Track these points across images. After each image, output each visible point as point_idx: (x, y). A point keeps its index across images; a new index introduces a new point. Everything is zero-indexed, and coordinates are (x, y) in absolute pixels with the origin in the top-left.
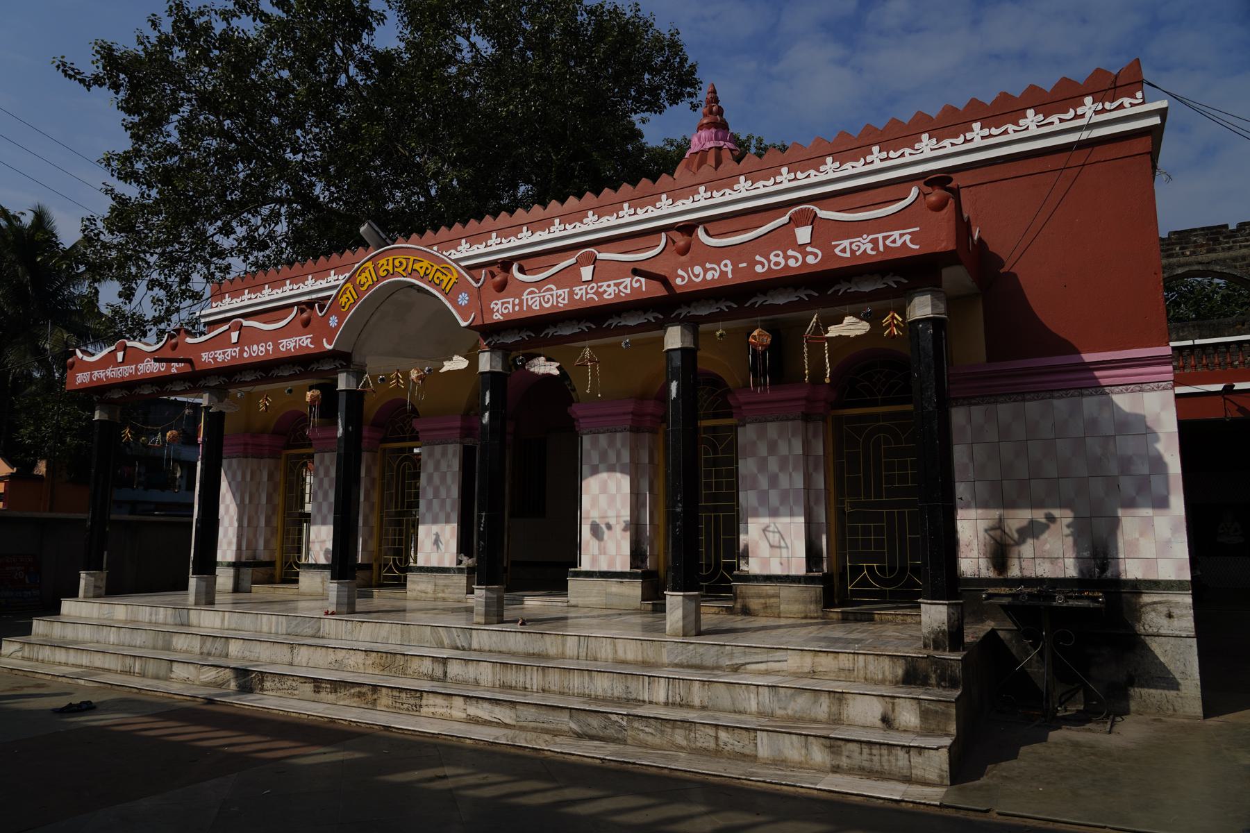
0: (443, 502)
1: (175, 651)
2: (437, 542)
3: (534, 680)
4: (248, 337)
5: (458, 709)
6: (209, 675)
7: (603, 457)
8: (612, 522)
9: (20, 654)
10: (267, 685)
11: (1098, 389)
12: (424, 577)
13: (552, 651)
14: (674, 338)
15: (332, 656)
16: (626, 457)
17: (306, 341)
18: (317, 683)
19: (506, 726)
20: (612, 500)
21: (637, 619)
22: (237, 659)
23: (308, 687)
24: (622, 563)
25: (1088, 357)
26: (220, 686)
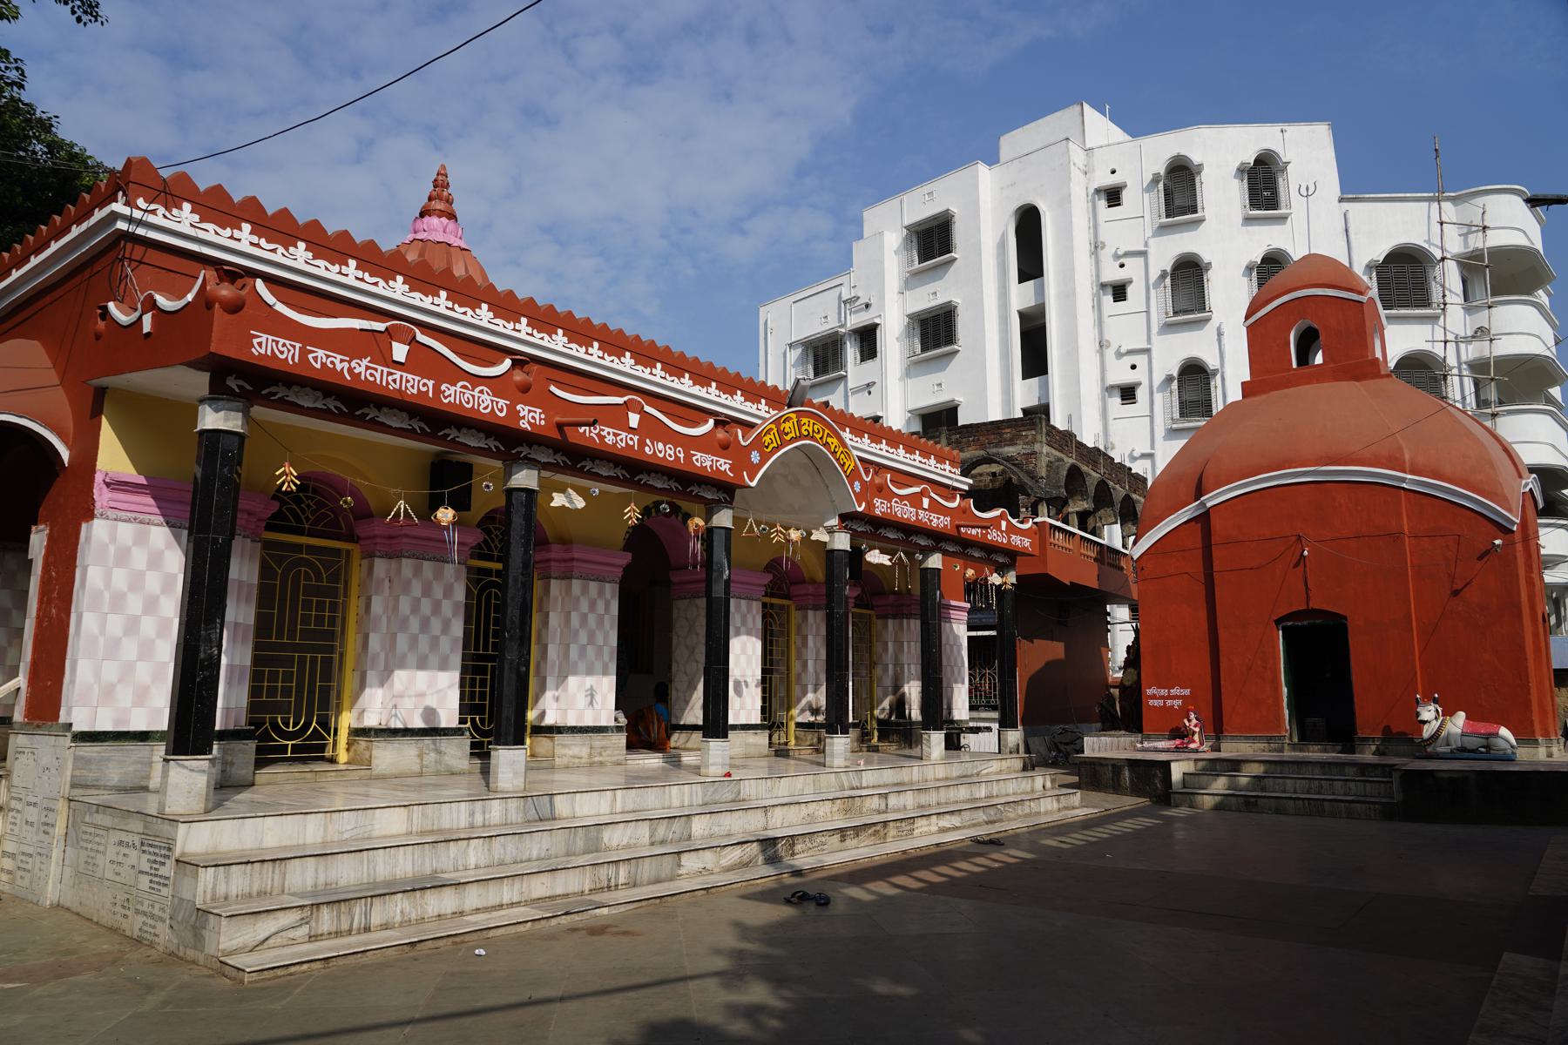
1: (608, 849)
3: (963, 793)
4: (649, 428)
5: (935, 824)
6: (735, 855)
9: (304, 930)
10: (798, 848)
11: (949, 619)
12: (578, 738)
14: (935, 561)
16: (759, 625)
17: (724, 465)
18: (842, 831)
19: (958, 828)
21: (764, 763)
22: (703, 838)
23: (837, 837)
24: (756, 719)
25: (953, 603)
26: (747, 865)
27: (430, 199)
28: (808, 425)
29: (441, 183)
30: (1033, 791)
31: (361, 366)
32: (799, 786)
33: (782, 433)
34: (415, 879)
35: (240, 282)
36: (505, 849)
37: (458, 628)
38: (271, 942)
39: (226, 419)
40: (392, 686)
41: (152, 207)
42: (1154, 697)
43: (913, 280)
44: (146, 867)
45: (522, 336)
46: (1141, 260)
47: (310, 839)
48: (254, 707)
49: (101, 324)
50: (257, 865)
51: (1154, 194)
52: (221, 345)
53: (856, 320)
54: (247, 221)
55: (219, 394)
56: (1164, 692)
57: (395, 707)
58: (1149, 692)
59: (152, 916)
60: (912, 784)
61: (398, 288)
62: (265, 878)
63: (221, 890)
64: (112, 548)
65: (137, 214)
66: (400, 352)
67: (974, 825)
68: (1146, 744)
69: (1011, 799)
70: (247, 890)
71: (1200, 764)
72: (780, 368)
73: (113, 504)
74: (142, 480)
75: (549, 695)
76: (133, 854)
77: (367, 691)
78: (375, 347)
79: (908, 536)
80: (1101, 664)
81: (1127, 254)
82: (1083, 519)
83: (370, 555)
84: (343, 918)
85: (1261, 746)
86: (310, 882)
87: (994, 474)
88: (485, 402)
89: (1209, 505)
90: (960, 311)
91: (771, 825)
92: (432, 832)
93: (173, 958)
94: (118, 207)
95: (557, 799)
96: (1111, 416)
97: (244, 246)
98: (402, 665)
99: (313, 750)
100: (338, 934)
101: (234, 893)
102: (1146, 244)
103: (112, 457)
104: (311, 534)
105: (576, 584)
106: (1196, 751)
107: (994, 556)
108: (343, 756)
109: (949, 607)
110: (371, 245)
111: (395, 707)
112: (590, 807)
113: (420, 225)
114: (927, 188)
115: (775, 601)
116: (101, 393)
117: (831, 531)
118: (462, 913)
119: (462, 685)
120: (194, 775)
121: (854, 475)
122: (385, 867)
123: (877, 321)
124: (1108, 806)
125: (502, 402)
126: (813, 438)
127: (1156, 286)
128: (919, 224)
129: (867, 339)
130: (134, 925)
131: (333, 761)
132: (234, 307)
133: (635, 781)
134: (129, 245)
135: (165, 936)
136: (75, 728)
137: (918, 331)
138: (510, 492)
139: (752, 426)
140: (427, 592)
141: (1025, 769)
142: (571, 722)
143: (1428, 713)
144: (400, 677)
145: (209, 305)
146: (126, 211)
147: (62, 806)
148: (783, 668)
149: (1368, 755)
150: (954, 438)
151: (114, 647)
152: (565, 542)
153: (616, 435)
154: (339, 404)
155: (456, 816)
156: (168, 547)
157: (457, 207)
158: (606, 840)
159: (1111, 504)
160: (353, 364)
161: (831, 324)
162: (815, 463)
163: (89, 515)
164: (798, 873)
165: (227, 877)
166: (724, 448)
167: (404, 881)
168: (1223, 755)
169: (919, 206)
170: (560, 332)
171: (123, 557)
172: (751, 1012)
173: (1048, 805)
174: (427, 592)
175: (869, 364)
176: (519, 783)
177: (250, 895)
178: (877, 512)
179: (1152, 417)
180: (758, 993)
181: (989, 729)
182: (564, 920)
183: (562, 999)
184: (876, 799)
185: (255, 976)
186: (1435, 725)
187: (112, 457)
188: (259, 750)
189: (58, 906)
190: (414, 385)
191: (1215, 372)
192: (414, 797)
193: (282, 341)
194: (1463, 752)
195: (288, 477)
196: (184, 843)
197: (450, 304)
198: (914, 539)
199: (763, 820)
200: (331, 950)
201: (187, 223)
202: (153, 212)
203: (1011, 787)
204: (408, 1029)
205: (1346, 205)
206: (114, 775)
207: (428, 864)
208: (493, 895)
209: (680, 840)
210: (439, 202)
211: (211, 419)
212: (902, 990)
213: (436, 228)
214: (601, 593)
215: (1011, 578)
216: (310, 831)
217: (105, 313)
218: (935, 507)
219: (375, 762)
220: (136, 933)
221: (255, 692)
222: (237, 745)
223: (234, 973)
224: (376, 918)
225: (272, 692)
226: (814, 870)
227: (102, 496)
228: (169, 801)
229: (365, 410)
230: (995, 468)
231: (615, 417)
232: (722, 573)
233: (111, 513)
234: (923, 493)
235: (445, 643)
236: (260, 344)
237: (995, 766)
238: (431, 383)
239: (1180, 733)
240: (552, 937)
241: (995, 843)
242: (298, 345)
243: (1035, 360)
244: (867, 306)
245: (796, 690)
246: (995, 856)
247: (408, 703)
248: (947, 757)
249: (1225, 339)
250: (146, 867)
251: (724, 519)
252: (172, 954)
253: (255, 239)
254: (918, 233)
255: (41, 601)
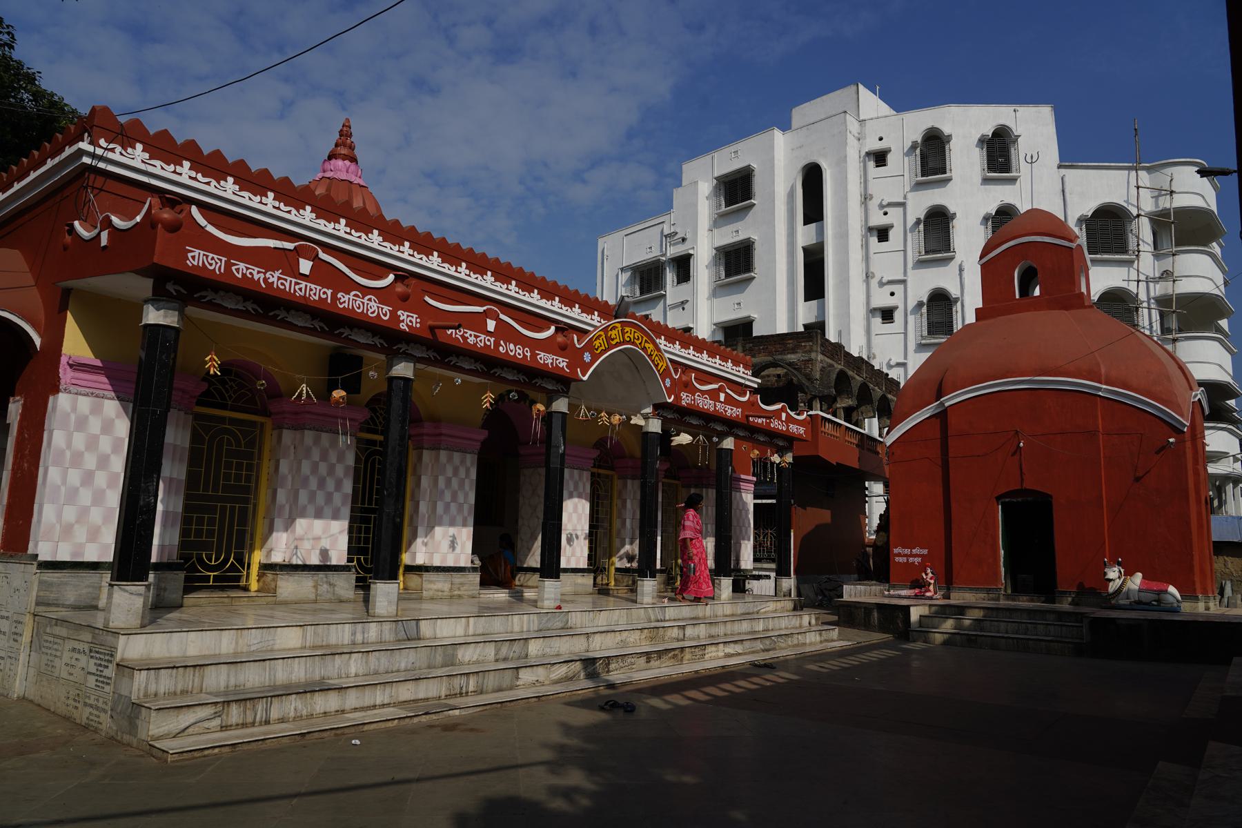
0: (460, 507)
1: (461, 664)
2: (453, 545)
3: (745, 626)
4: (504, 332)
5: (722, 650)
6: (562, 671)
7: (576, 487)
8: (579, 533)
9: (217, 722)
10: (612, 666)
11: (739, 490)
12: (441, 576)
13: (701, 615)
14: (729, 443)
15: (618, 637)
17: (562, 363)
18: (648, 655)
19: (739, 654)
20: (579, 519)
21: (589, 599)
22: (537, 656)
23: (643, 660)
24: (583, 563)
25: (743, 477)
26: (571, 679)
27: (337, 145)
28: (630, 333)
29: (345, 133)
30: (801, 627)
31: (274, 277)
32: (615, 618)
33: (609, 339)
34: (307, 684)
35: (178, 208)
36: (379, 662)
37: (348, 487)
38: (190, 730)
39: (165, 316)
40: (294, 532)
41: (111, 146)
42: (899, 555)
43: (721, 220)
44: (93, 669)
45: (405, 256)
46: (901, 209)
47: (224, 650)
48: (183, 545)
49: (68, 238)
50: (181, 670)
51: (912, 158)
52: (163, 256)
53: (673, 251)
54: (187, 159)
55: (160, 297)
56: (907, 551)
57: (296, 548)
58: (896, 551)
59: (97, 708)
60: (705, 618)
61: (307, 216)
62: (187, 680)
63: (152, 688)
64: (73, 417)
65: (99, 151)
66: (305, 266)
67: (753, 652)
68: (892, 592)
69: (783, 632)
70: (172, 689)
71: (933, 609)
72: (612, 286)
73: (74, 381)
74: (98, 363)
75: (419, 541)
76: (84, 659)
77: (274, 534)
78: (286, 261)
79: (708, 423)
80: (860, 528)
81: (890, 205)
82: (849, 414)
83: (279, 427)
84: (248, 712)
85: (982, 596)
86: (223, 684)
87: (779, 376)
88: (372, 308)
89: (947, 404)
90: (757, 246)
91: (592, 647)
92: (322, 647)
93: (112, 740)
94: (84, 145)
95: (422, 623)
96: (873, 333)
97: (184, 179)
98: (303, 515)
99: (231, 580)
100: (244, 725)
101: (162, 691)
102: (905, 197)
103: (75, 344)
104: (233, 409)
105: (443, 455)
106: (931, 598)
107: (776, 441)
108: (254, 586)
109: (740, 480)
110: (286, 181)
111: (296, 548)
112: (449, 630)
113: (327, 166)
114: (733, 148)
115: (601, 471)
116: (67, 292)
117: (646, 417)
118: (343, 712)
119: (350, 532)
120: (133, 597)
121: (666, 374)
122: (283, 674)
123: (691, 252)
124: (860, 640)
125: (386, 308)
126: (633, 343)
127: (912, 230)
128: (726, 176)
129: (683, 266)
130: (83, 714)
131: (246, 589)
132: (174, 227)
133: (487, 611)
134: (92, 176)
135: (106, 723)
136: (40, 558)
137: (723, 261)
138: (391, 380)
139: (586, 332)
140: (324, 457)
141: (795, 609)
142: (437, 563)
143: (1113, 573)
144: (301, 524)
145: (153, 226)
146: (90, 148)
147: (28, 619)
148: (606, 525)
149: (1065, 605)
150: (748, 346)
151: (72, 495)
152: (436, 420)
153: (476, 337)
154: (255, 307)
155: (341, 635)
156: (118, 416)
157: (357, 152)
158: (460, 656)
159: (870, 402)
160: (268, 275)
161: (655, 253)
162: (634, 363)
163: (56, 390)
164: (611, 686)
165: (157, 679)
166: (562, 350)
167: (298, 685)
168: (952, 602)
169: (726, 161)
170: (436, 254)
171: (82, 424)
172: (568, 793)
173: (813, 638)
174: (324, 457)
175: (684, 286)
176: (392, 609)
177: (175, 693)
178: (683, 403)
179: (905, 334)
180: (575, 778)
181: (768, 577)
182: (424, 719)
183: (418, 780)
184: (676, 630)
185: (176, 757)
186: (1118, 582)
187: (75, 344)
188: (187, 579)
189: (23, 699)
190: (316, 293)
191: (956, 300)
192: (309, 619)
193: (211, 255)
194: (1139, 604)
195: (213, 365)
196: (124, 650)
197: (348, 230)
198: (712, 425)
199: (585, 644)
200: (238, 737)
201: (139, 159)
202: (112, 150)
203: (784, 623)
204: (295, 801)
205: (1063, 171)
206: (71, 596)
207: (317, 672)
208: (368, 698)
209: (519, 658)
210: (344, 148)
211: (153, 316)
212: (687, 779)
213: (340, 169)
214: (463, 462)
215: (789, 458)
216: (225, 643)
217: (72, 230)
218: (729, 401)
219: (279, 591)
220: (84, 721)
221: (184, 533)
222: (169, 575)
223: (160, 753)
224: (275, 714)
225: (199, 533)
226: (624, 684)
227: (66, 375)
228: (112, 617)
229: (277, 312)
230: (780, 371)
231: (476, 322)
232: (559, 447)
233: (72, 388)
234: (721, 389)
235: (337, 498)
236: (193, 257)
237: (771, 606)
238: (329, 292)
239: (919, 584)
240: (414, 731)
241: (768, 666)
242: (224, 259)
243: (815, 287)
244: (684, 240)
245: (617, 542)
246: (767, 677)
247: (307, 545)
248: (733, 598)
249: (965, 274)
250: (93, 669)
251: (561, 405)
252: (112, 738)
253: (193, 174)
254: (725, 183)
255: (15, 457)
